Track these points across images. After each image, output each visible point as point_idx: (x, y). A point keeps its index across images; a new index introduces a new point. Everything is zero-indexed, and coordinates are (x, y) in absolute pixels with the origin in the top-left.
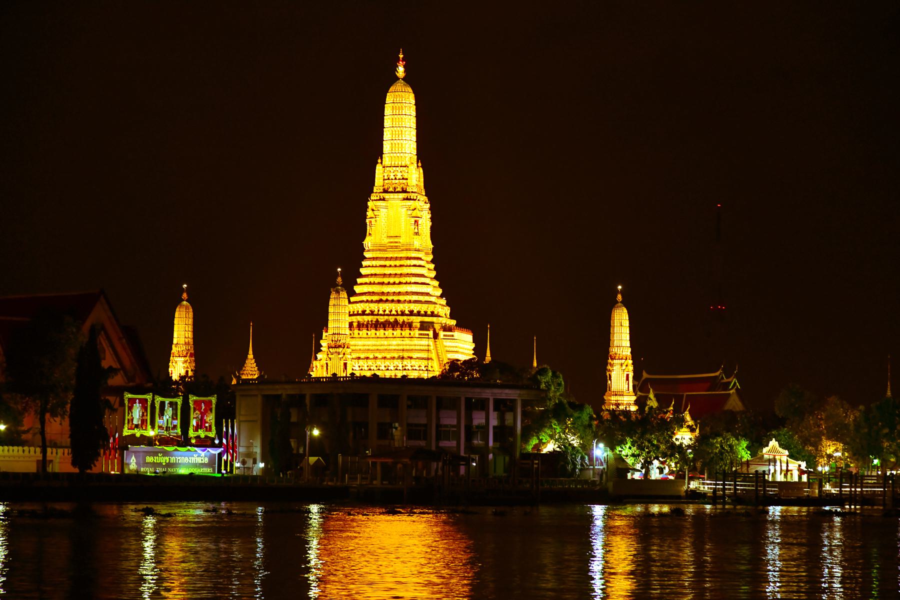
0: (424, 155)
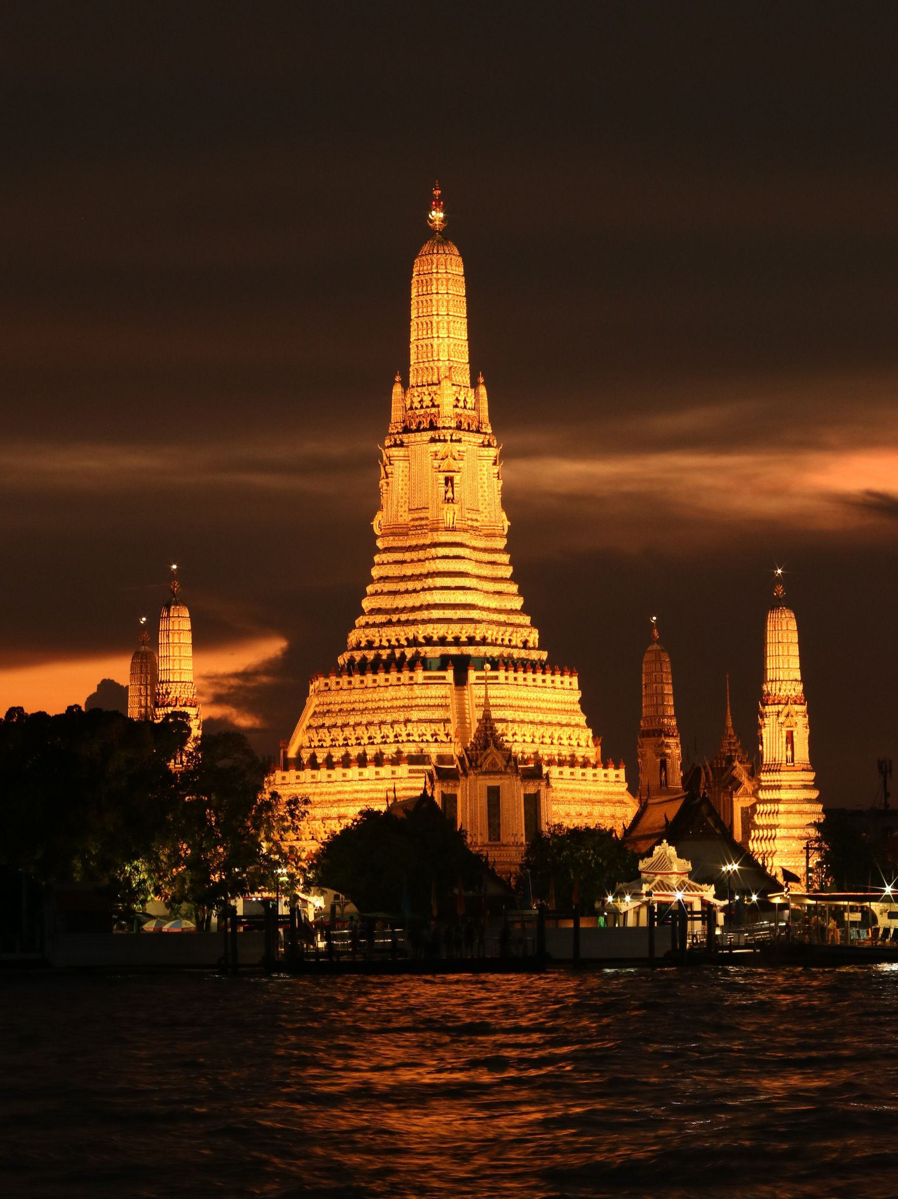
0: (484, 362)
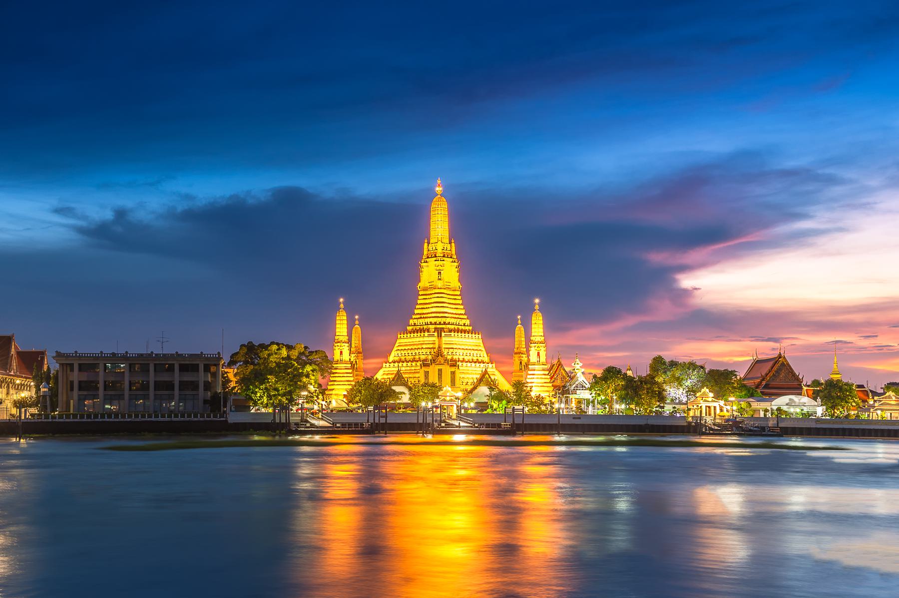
0: (454, 235)
